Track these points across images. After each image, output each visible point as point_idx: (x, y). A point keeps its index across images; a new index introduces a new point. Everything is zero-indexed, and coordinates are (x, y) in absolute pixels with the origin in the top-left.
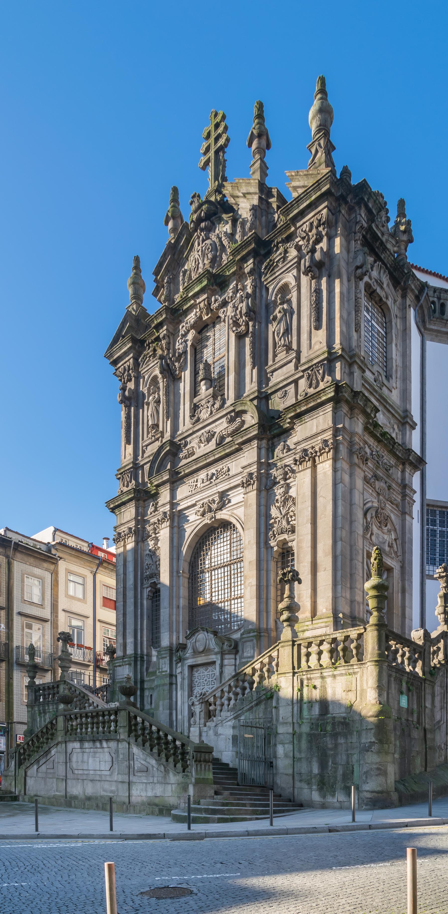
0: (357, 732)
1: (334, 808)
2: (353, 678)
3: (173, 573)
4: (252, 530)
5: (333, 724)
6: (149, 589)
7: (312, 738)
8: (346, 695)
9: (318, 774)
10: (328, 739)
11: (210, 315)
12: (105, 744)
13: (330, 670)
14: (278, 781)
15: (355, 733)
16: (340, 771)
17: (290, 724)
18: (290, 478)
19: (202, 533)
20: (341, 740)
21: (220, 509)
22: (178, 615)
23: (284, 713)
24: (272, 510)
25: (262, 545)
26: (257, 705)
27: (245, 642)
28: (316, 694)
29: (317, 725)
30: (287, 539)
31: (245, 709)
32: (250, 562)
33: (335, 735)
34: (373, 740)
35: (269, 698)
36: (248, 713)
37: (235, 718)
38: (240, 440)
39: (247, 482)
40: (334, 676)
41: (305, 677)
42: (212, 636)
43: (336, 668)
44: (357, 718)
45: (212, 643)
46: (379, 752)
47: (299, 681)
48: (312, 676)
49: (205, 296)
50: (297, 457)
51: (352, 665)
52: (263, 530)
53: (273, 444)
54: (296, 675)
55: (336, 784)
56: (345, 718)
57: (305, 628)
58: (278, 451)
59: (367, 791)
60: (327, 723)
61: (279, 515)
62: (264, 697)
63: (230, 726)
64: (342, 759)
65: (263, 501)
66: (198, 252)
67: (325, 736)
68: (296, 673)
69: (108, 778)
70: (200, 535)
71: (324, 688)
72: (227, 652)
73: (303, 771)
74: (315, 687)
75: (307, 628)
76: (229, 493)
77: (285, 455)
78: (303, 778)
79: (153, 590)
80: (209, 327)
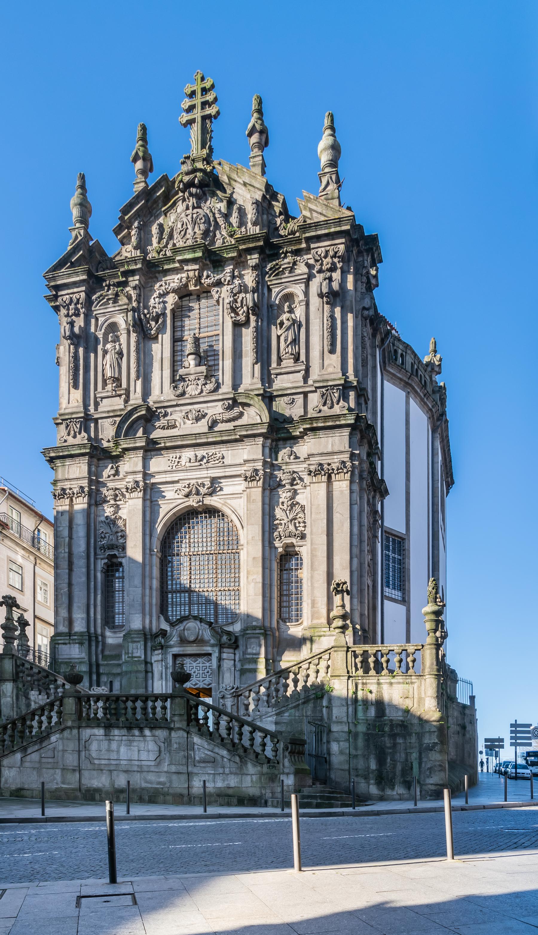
0: (416, 734)
1: (394, 800)
2: (410, 687)
3: (146, 550)
4: (257, 526)
5: (392, 726)
6: (106, 561)
7: (368, 737)
8: (403, 701)
9: (376, 770)
10: (386, 739)
11: (198, 287)
12: (147, 732)
13: (388, 678)
14: (333, 776)
15: (414, 735)
16: (399, 767)
17: (346, 723)
18: (297, 484)
19: (180, 513)
20: (400, 741)
21: (211, 494)
22: (151, 597)
23: (338, 712)
24: (276, 511)
25: (267, 544)
26: (304, 703)
27: (250, 638)
28: (372, 697)
29: (375, 726)
30: (295, 544)
31: (290, 706)
32: (254, 558)
33: (393, 736)
34: (436, 741)
35: (319, 698)
36: (293, 711)
37: (277, 714)
38: (244, 433)
39: (251, 477)
40: (391, 684)
41: (360, 681)
42: (207, 627)
43: (394, 677)
44: (416, 721)
45: (207, 634)
46: (441, 752)
47: (354, 684)
48: (368, 681)
49: (197, 267)
50: (312, 468)
51: (411, 676)
52: (267, 528)
53: (277, 445)
54: (351, 679)
55: (394, 778)
56: (402, 721)
57: (322, 633)
58: (283, 454)
59: (432, 784)
60: (385, 724)
61: (285, 517)
62: (313, 696)
63: (271, 722)
64: (401, 756)
65: (267, 500)
66: (187, 216)
67: (383, 736)
68: (352, 677)
69: (152, 769)
70: (177, 515)
71: (379, 692)
72: (226, 646)
73: (360, 767)
74: (371, 692)
75: (324, 634)
76: (221, 481)
77: (292, 461)
78: (360, 773)
79: (109, 562)
80: (191, 297)
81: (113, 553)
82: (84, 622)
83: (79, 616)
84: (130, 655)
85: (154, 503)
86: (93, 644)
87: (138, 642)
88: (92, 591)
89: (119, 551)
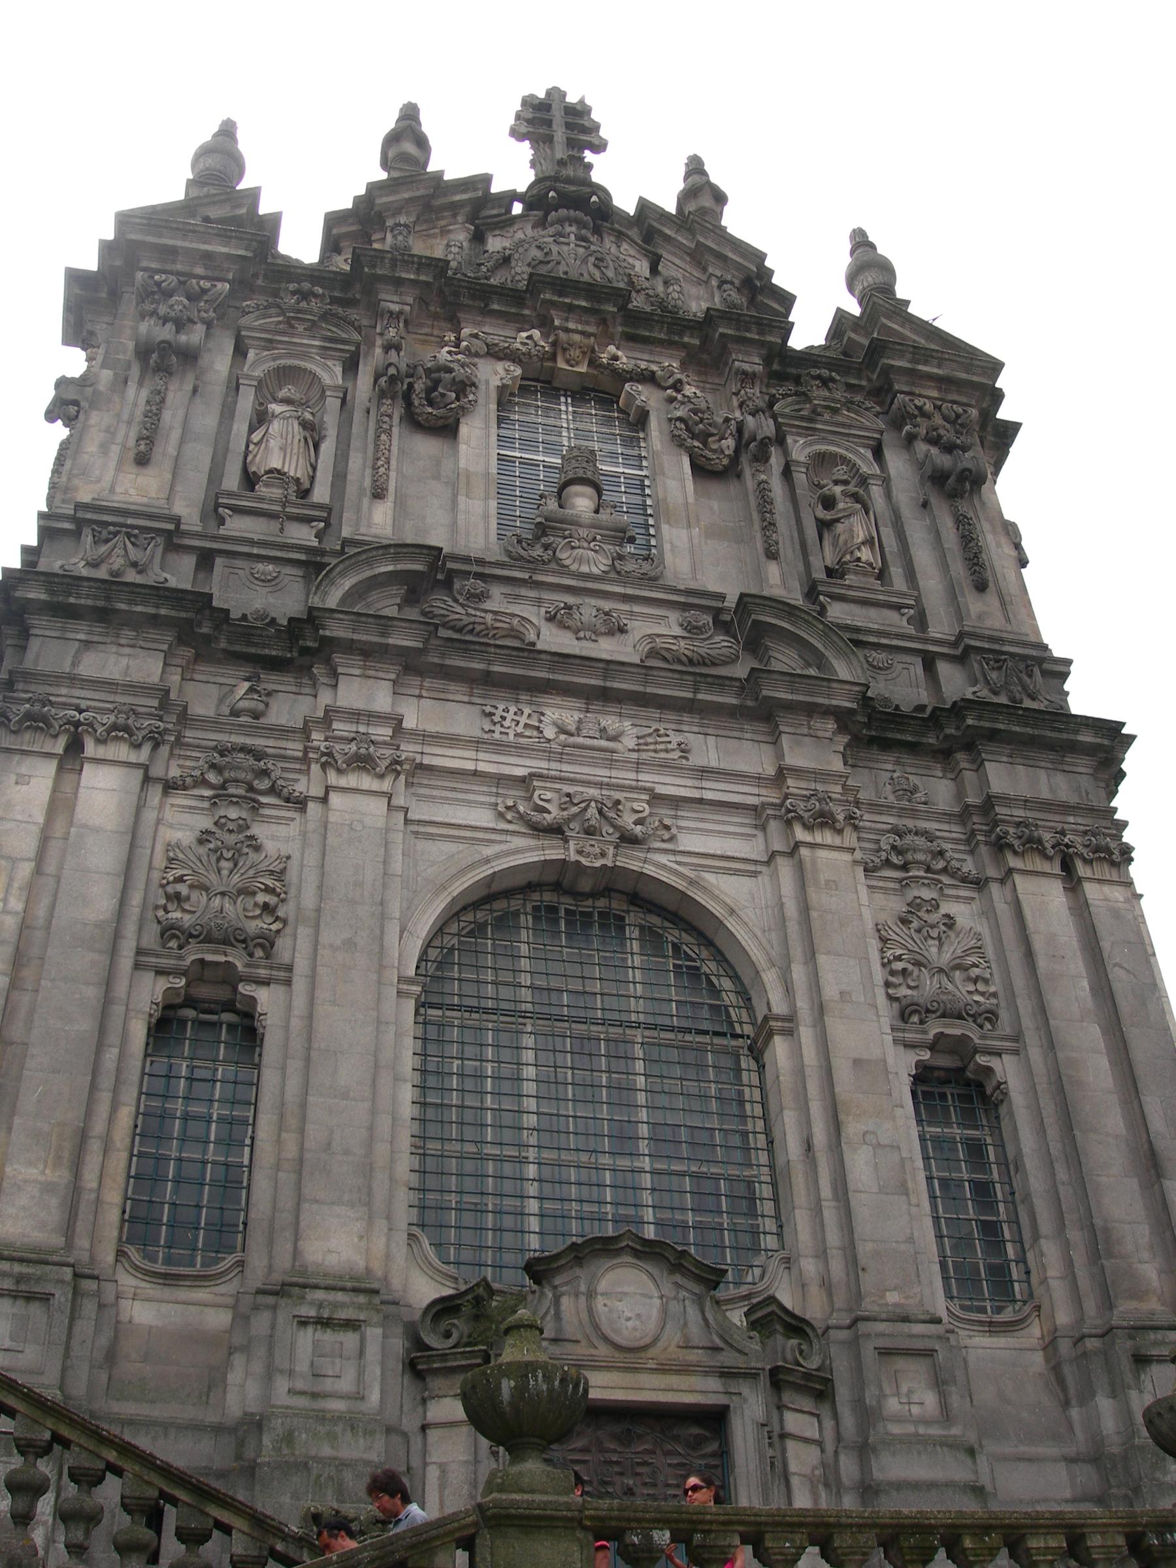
81: (222, 959)
82: (54, 1202)
83: (34, 1172)
84: (300, 1385)
85: (415, 828)
86: (89, 1307)
87: (351, 1325)
88: (106, 1082)
89: (251, 955)
